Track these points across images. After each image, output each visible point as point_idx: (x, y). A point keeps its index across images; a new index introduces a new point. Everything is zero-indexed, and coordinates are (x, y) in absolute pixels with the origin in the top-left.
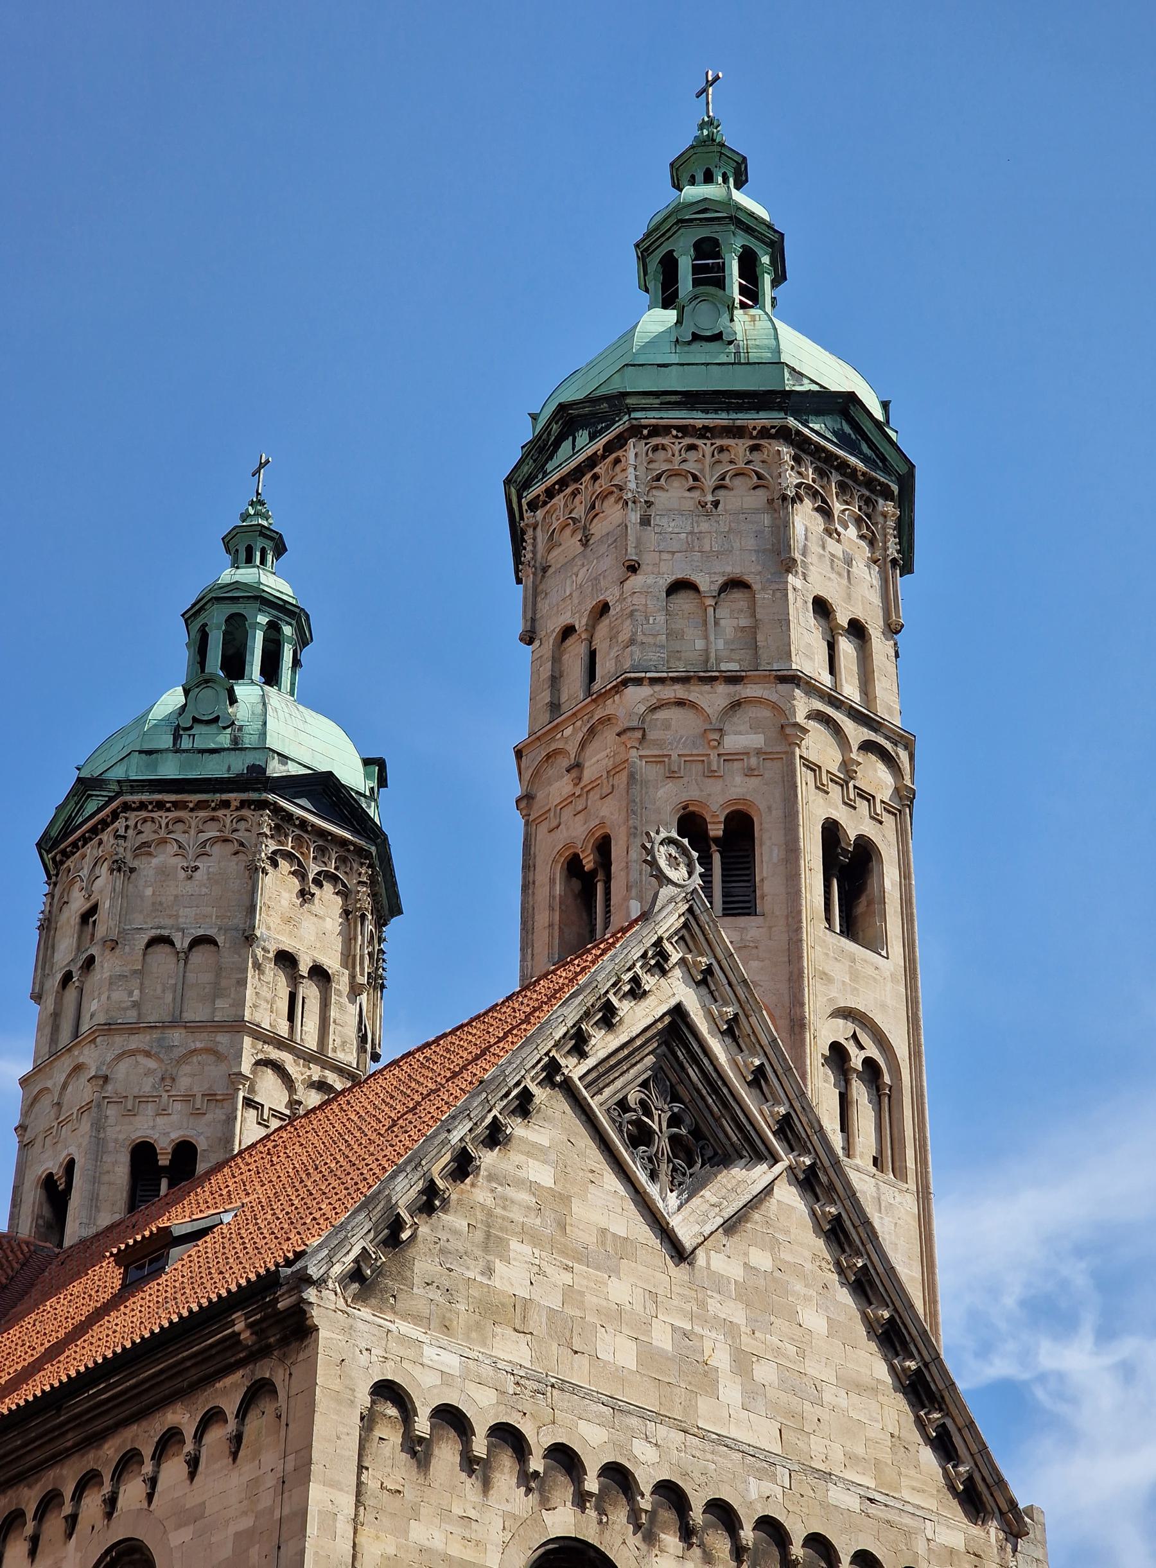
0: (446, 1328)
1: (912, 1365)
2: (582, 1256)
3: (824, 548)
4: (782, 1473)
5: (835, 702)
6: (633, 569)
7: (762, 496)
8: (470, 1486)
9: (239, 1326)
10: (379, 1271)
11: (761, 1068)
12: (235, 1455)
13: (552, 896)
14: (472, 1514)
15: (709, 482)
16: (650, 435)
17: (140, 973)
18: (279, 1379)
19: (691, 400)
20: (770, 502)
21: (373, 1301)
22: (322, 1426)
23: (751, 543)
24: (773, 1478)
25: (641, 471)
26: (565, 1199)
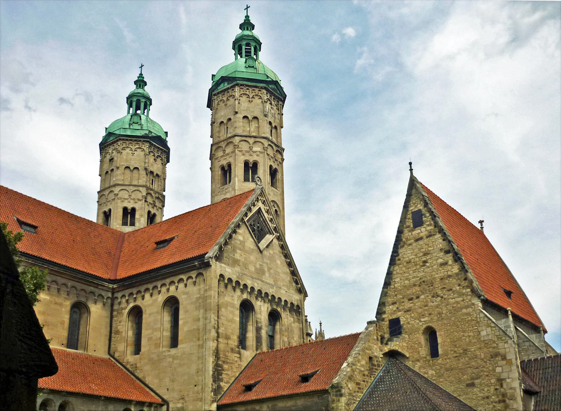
0: (228, 265)
1: (292, 269)
3: (271, 111)
4: (275, 288)
6: (236, 113)
7: (260, 100)
14: (233, 295)
15: (251, 96)
16: (240, 86)
17: (123, 173)
20: (262, 102)
24: (273, 289)
25: (238, 93)
26: (245, 242)
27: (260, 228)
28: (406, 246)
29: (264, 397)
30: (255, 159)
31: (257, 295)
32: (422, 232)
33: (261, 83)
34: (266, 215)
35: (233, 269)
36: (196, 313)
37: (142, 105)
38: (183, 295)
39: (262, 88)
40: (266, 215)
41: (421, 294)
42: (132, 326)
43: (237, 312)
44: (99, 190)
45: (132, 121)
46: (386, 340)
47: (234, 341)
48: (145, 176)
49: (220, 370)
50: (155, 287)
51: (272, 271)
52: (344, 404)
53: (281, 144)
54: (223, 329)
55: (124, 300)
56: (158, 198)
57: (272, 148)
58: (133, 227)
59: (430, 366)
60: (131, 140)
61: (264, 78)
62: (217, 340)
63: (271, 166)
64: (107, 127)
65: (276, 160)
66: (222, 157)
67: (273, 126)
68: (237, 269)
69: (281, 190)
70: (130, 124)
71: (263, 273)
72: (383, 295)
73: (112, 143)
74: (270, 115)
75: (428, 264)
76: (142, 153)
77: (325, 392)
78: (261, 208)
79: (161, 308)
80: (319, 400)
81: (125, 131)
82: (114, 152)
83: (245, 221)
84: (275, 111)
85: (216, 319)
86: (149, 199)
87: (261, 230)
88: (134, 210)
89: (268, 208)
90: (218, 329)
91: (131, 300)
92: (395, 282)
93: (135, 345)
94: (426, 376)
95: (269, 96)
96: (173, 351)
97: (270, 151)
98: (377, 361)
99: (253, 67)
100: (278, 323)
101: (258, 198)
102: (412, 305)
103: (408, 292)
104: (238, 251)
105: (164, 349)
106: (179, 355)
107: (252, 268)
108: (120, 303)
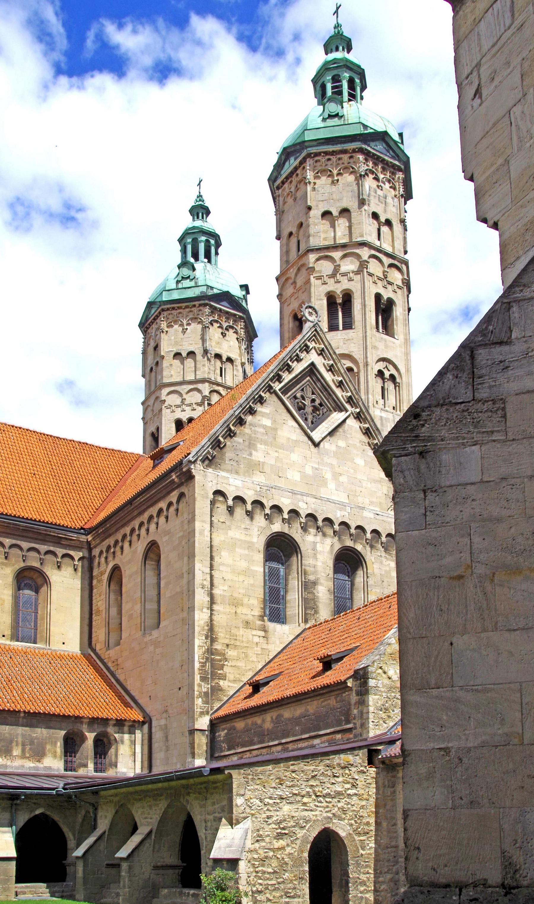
0: (237, 473)
2: (282, 447)
8: (247, 519)
9: (174, 477)
10: (214, 457)
11: (341, 381)
12: (177, 514)
13: (289, 328)
14: (248, 527)
18: (186, 492)
21: (213, 467)
22: (198, 505)
24: (345, 510)
26: (276, 429)
27: (317, 402)
31: (306, 524)
38: (165, 536)
43: (260, 557)
54: (226, 588)
55: (103, 560)
66: (292, 295)
68: (259, 478)
71: (324, 482)
79: (140, 563)
80: (337, 702)
83: (275, 393)
87: (321, 405)
89: (331, 362)
90: (211, 589)
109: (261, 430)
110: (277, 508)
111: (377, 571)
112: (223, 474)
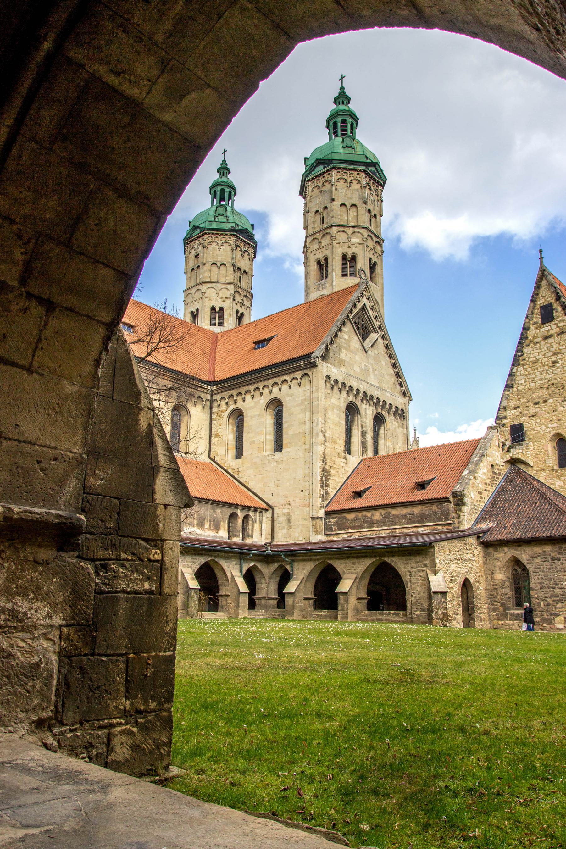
0: (334, 365)
5: (372, 232)
6: (333, 200)
7: (359, 185)
8: (339, 392)
15: (349, 181)
18: (310, 373)
19: (346, 162)
23: (357, 196)
26: (349, 341)
28: (532, 344)
29: (377, 504)
30: (353, 251)
32: (552, 329)
33: (359, 165)
34: (370, 311)
35: (339, 370)
36: (301, 416)
37: (227, 195)
39: (360, 171)
40: (370, 311)
41: (549, 397)
42: (233, 429)
43: (343, 416)
44: (185, 289)
45: (217, 212)
46: (508, 446)
47: (341, 446)
48: (233, 272)
49: (328, 476)
50: (257, 389)
51: (377, 372)
52: (466, 514)
53: (380, 234)
54: (330, 433)
55: (223, 403)
56: (246, 296)
57: (372, 238)
58: (221, 327)
59: (558, 476)
60: (217, 234)
61: (364, 160)
62: (324, 445)
63: (370, 259)
64: (191, 220)
65: (376, 253)
66: (318, 249)
67: (373, 214)
68: (343, 369)
69: (380, 285)
70: (215, 217)
71: (369, 375)
72: (504, 398)
73: (198, 238)
74: (369, 202)
75: (558, 365)
76: (229, 248)
77: (445, 500)
78: (366, 304)
81: (211, 225)
82: (200, 247)
84: (374, 197)
85: (323, 422)
86: (238, 298)
88: (221, 309)
89: (373, 304)
91: (231, 403)
92: (518, 384)
93: (236, 449)
94: (552, 487)
95: (368, 180)
96: (278, 455)
97: (370, 243)
98: (498, 470)
99: (351, 147)
100: (382, 428)
101: (362, 294)
102: (538, 409)
103: (534, 396)
104: (343, 350)
105: (268, 453)
106: (285, 459)
107: (357, 369)
108: (219, 406)
109: (344, 341)
110: (351, 387)
111: (391, 428)
112: (329, 365)
